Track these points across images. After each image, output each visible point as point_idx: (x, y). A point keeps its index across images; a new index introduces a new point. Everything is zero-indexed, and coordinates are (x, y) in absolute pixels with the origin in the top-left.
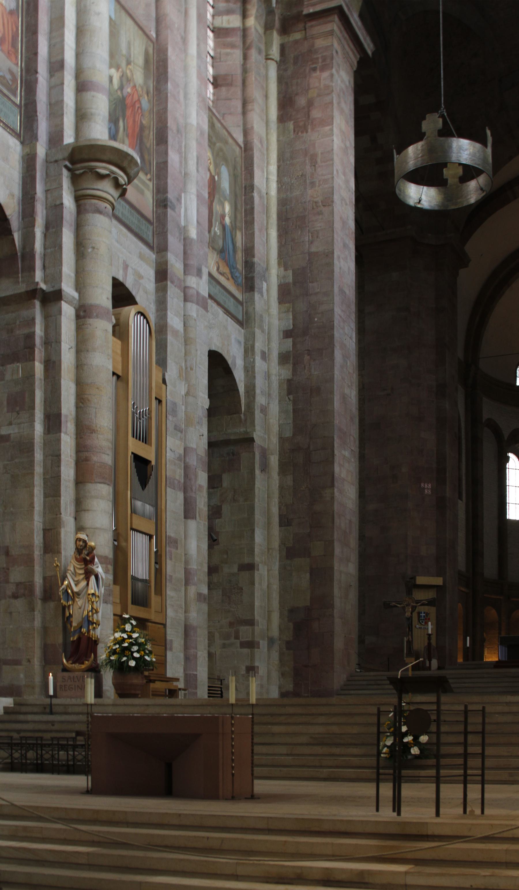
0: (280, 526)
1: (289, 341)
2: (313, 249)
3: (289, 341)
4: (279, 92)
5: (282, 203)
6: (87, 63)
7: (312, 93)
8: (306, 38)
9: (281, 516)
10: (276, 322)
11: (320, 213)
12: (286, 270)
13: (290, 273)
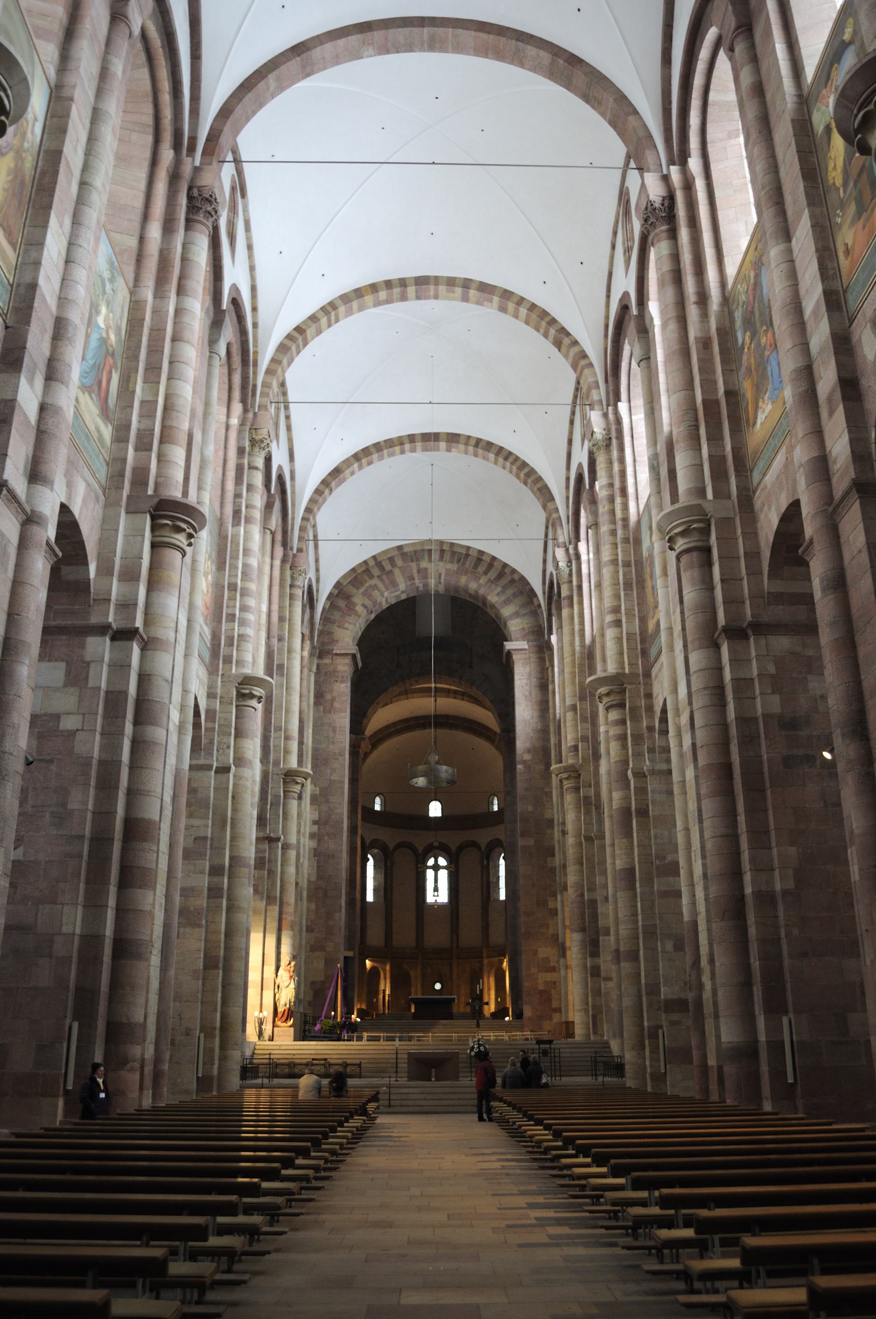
0: (307, 931)
1: (316, 828)
2: (332, 778)
3: (316, 828)
4: (315, 689)
5: (315, 750)
6: (290, 727)
7: (335, 694)
8: (332, 664)
9: (307, 926)
10: (308, 815)
11: (337, 759)
12: (315, 786)
13: (318, 789)
